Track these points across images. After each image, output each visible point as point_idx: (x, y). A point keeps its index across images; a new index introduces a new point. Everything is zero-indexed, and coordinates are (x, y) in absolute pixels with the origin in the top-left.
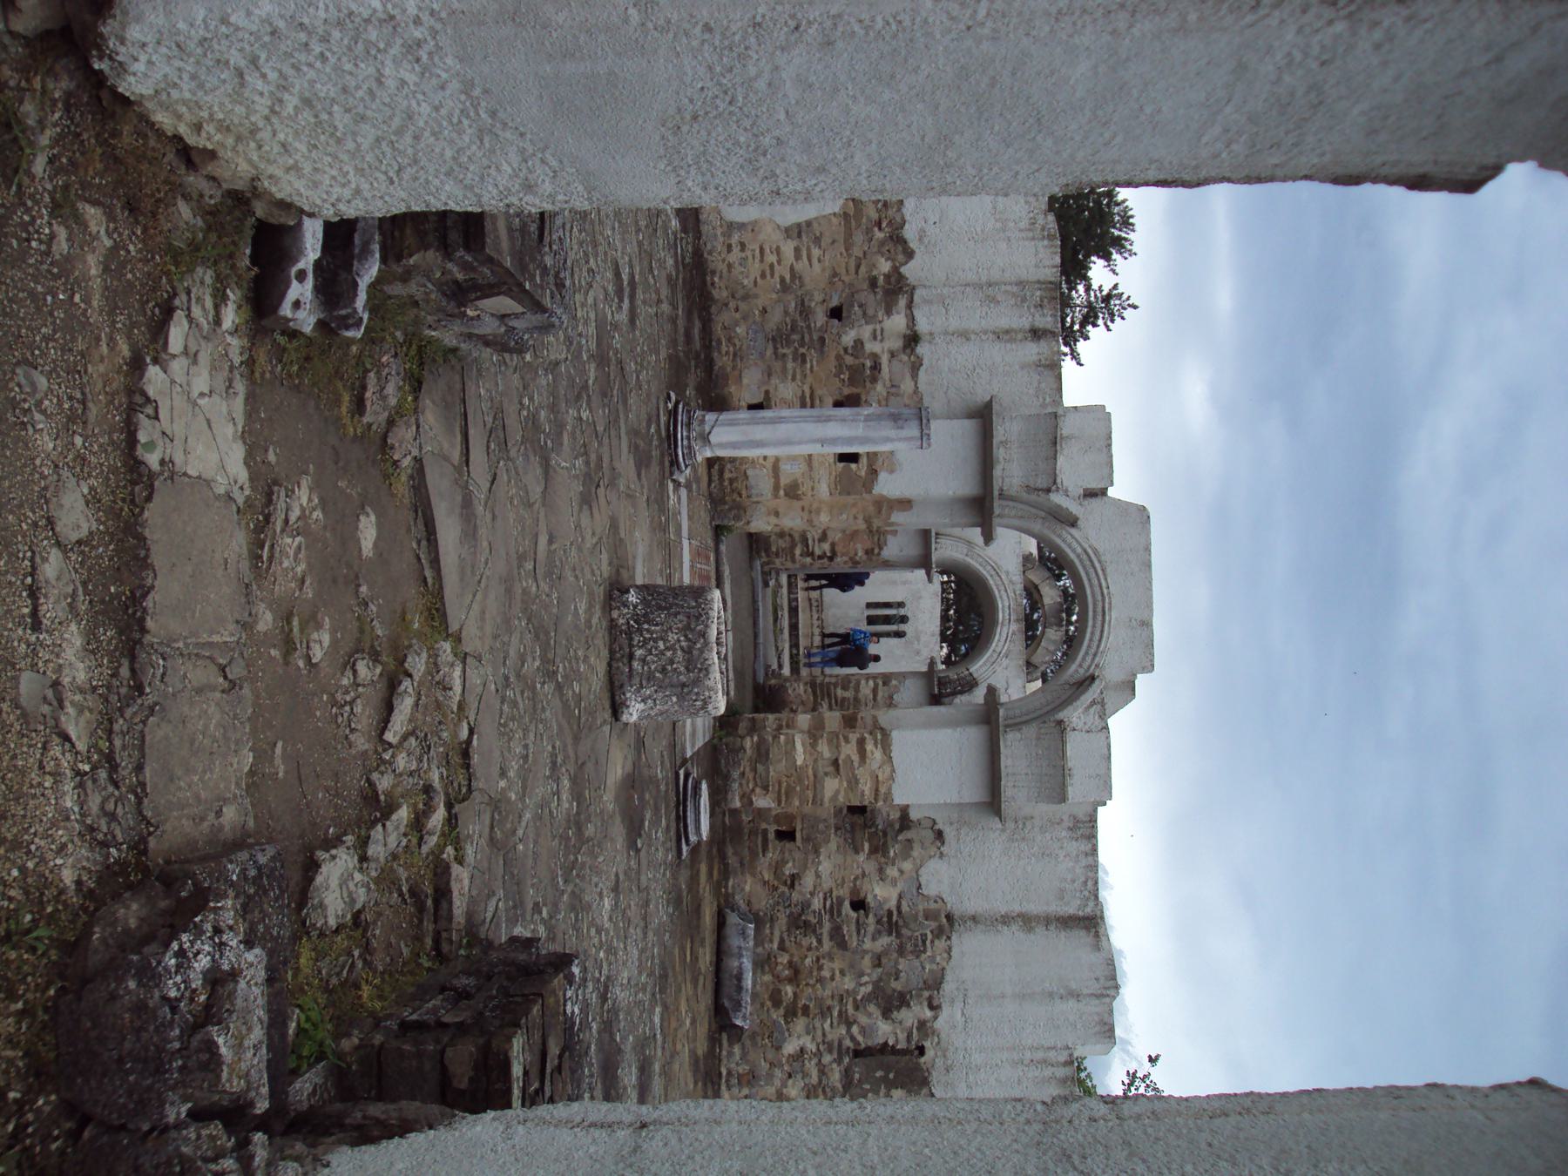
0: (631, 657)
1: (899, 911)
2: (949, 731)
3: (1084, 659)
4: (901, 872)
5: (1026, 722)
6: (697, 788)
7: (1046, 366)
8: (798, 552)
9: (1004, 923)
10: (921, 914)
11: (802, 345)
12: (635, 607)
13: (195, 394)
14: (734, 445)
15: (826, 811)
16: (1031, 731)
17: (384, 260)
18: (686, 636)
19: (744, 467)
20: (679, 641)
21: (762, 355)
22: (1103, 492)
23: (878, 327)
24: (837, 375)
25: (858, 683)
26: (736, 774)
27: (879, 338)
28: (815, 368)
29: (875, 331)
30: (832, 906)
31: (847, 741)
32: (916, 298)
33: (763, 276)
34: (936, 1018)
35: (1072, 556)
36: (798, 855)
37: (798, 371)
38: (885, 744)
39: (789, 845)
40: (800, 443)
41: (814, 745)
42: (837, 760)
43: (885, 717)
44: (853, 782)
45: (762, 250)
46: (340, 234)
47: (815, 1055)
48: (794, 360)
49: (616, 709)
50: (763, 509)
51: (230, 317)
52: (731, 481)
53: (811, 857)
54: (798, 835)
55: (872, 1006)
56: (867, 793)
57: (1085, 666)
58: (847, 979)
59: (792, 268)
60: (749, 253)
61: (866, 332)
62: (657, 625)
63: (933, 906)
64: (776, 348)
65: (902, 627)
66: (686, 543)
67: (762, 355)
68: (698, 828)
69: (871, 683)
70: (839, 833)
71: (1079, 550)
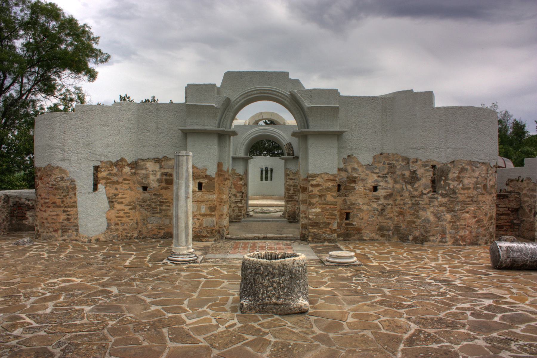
0: (276, 304)
3: (283, 98)
8: (240, 205)
18: (266, 276)
20: (268, 280)
23: (151, 173)
25: (288, 185)
28: (165, 198)
29: (152, 174)
30: (376, 199)
31: (312, 191)
33: (129, 217)
34: (421, 160)
35: (243, 101)
36: (355, 212)
37: (166, 204)
38: (314, 176)
39: (351, 215)
40: (187, 207)
41: (313, 204)
42: (319, 196)
43: (303, 176)
44: (328, 189)
45: (117, 217)
47: (434, 208)
48: (162, 206)
49: (302, 312)
50: (219, 221)
54: (348, 211)
55: (415, 185)
58: (404, 195)
59: (126, 205)
60: (119, 222)
61: (152, 177)
62: (260, 290)
64: (157, 213)
65: (269, 169)
66: (229, 256)
69: (288, 180)
70: (347, 195)
71: (241, 98)
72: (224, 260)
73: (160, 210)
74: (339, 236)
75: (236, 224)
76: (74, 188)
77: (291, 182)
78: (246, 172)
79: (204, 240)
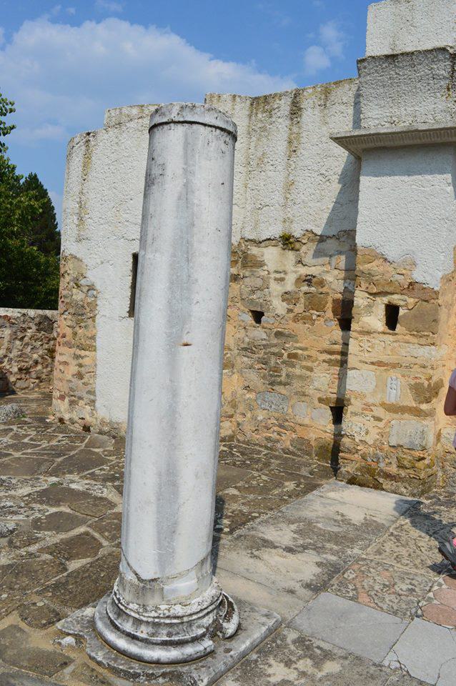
7: (326, 99)
11: (281, 356)
19: (386, 447)
23: (273, 275)
27: (282, 275)
29: (276, 279)
37: (304, 363)
40: (174, 393)
48: (293, 366)
52: (401, 466)
61: (276, 288)
64: (280, 383)
67: (285, 398)
73: (288, 375)
76: (93, 306)
79: (387, 484)
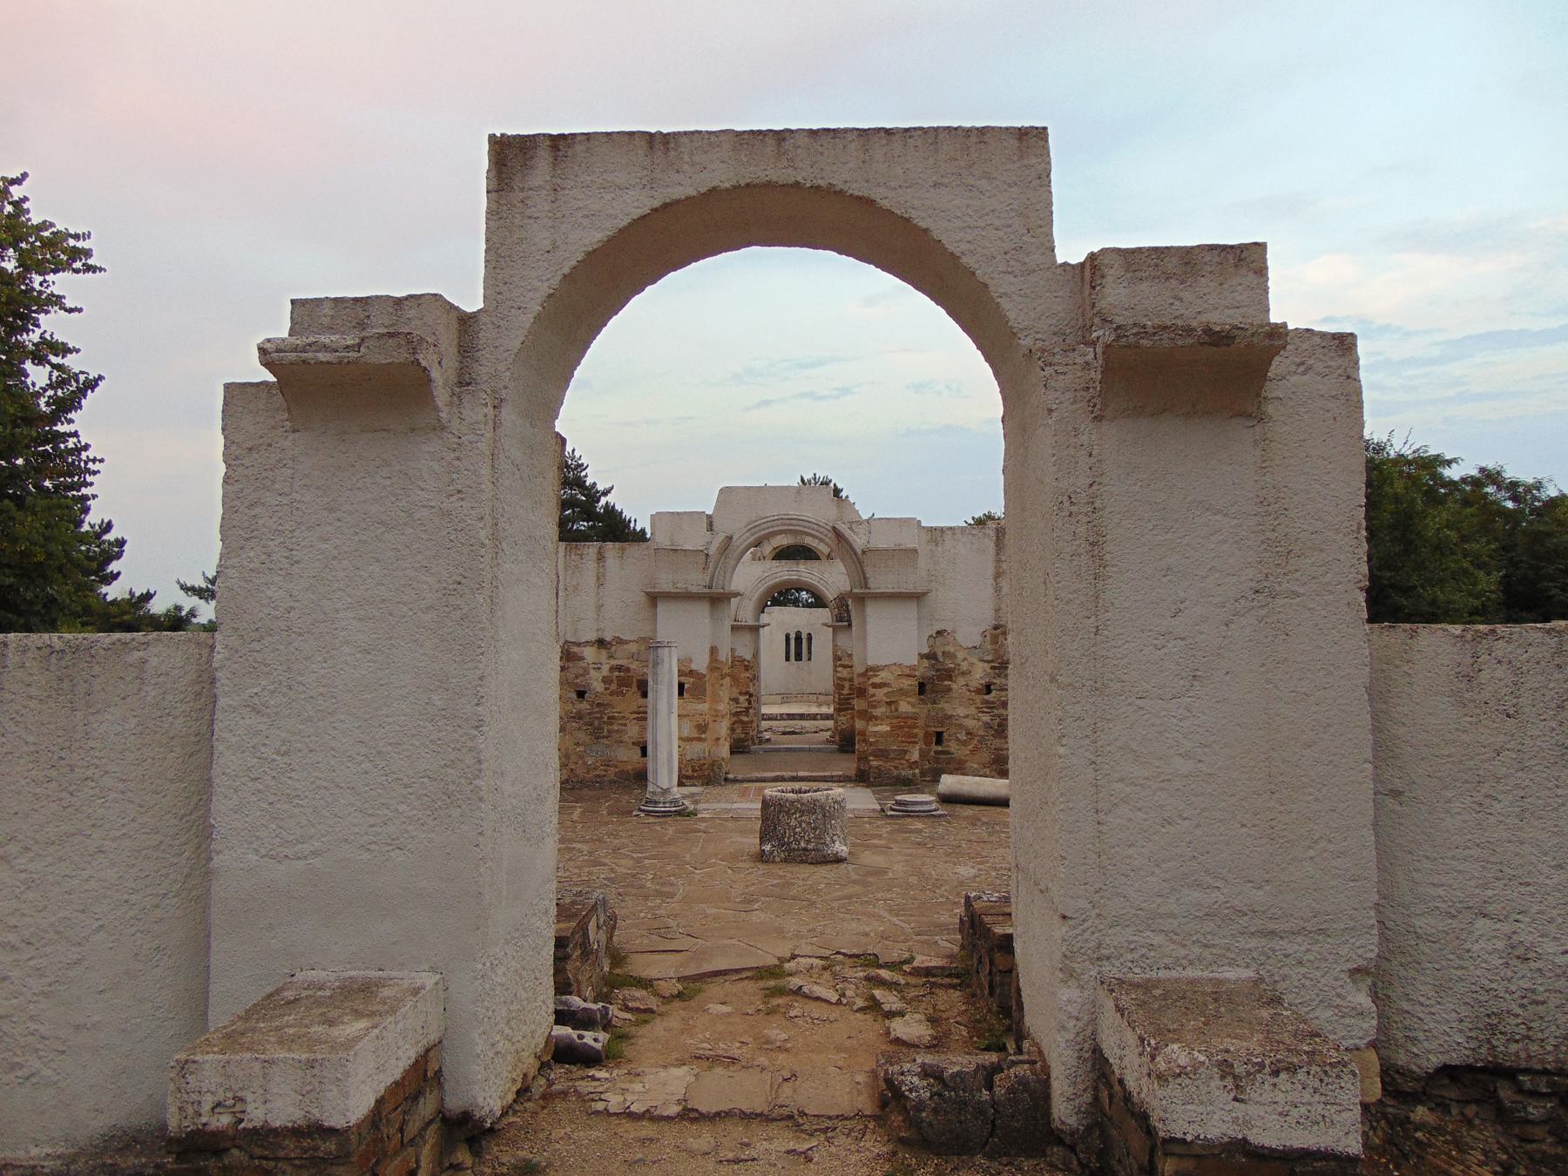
0: (805, 849)
1: (992, 661)
2: (868, 627)
4: (964, 659)
5: (864, 574)
6: (899, 803)
8: (745, 719)
9: (1000, 590)
10: (994, 647)
12: (773, 846)
13: (642, 1089)
14: (670, 773)
15: (922, 711)
16: (869, 572)
17: (570, 994)
18: (793, 814)
21: (607, 746)
22: (709, 517)
23: (592, 666)
24: (624, 695)
25: (839, 678)
26: (895, 773)
30: (988, 708)
31: (874, 695)
32: (573, 640)
36: (953, 730)
38: (875, 669)
40: (670, 728)
41: (876, 718)
43: (859, 669)
44: (903, 692)
46: (562, 1017)
48: (612, 724)
49: (839, 860)
51: (603, 1074)
53: (954, 722)
54: (939, 730)
56: (910, 682)
57: (826, 532)
63: (988, 638)
64: (603, 737)
65: (804, 636)
67: (607, 746)
68: (926, 803)
69: (840, 669)
72: (727, 811)
74: (923, 774)
75: (740, 756)
77: (844, 673)
78: (756, 655)
